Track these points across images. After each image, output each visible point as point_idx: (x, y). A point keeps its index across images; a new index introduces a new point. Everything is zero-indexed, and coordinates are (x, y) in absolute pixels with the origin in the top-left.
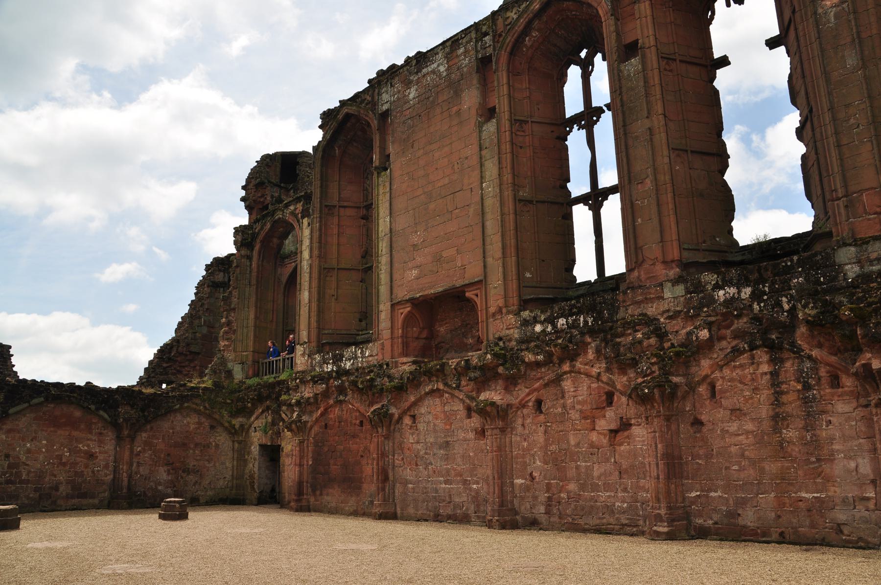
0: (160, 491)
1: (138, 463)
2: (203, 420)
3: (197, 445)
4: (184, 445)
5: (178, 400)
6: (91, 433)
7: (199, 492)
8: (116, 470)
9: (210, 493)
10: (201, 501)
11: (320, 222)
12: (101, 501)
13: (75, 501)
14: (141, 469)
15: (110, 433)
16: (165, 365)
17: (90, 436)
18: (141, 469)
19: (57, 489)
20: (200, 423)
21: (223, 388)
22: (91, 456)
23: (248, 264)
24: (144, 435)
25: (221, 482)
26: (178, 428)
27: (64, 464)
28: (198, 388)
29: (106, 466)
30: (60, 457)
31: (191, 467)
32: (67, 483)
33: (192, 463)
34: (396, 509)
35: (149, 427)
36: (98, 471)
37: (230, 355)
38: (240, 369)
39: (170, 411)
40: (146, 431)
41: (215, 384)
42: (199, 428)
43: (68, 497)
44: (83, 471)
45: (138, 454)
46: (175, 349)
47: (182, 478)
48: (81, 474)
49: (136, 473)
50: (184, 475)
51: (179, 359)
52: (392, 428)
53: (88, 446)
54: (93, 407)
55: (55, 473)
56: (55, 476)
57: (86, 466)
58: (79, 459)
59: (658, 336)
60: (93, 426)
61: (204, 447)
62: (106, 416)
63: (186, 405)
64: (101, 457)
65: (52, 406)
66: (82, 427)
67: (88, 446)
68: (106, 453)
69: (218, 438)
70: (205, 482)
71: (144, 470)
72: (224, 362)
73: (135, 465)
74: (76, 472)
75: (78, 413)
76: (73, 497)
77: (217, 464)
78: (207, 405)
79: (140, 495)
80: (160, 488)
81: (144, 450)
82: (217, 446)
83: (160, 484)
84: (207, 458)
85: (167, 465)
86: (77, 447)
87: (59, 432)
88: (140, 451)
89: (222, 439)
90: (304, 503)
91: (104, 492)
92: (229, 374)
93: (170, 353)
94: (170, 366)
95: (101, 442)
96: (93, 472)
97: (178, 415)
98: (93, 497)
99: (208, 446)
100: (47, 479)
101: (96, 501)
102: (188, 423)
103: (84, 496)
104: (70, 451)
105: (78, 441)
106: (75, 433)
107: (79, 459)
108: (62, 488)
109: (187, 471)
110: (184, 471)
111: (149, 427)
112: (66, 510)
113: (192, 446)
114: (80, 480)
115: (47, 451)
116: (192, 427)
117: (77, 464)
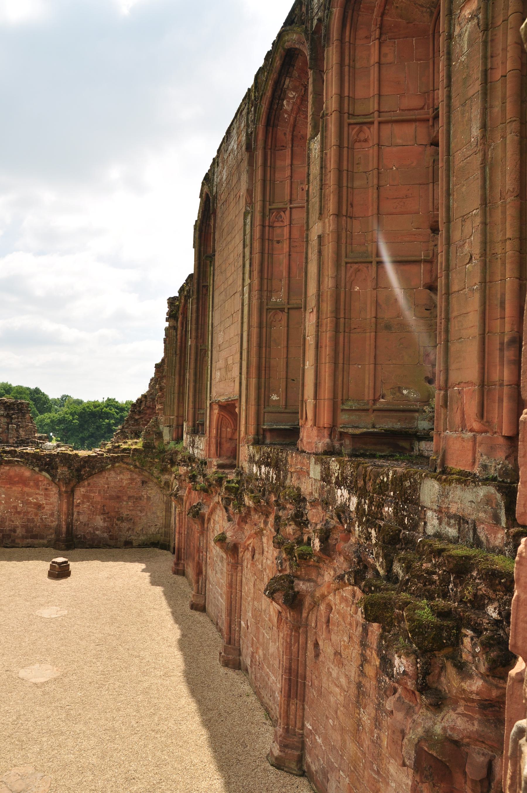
0: (97, 535)
1: (78, 512)
2: (135, 476)
3: (130, 497)
4: (118, 497)
5: (111, 460)
6: (38, 489)
7: (132, 537)
8: (59, 519)
9: (142, 538)
10: (134, 544)
11: (198, 303)
12: (49, 541)
13: (29, 541)
14: (81, 517)
15: (54, 489)
16: (137, 417)
17: (38, 491)
18: (81, 517)
19: (15, 531)
20: (132, 479)
21: (154, 448)
22: (39, 506)
23: (175, 334)
24: (82, 489)
25: (153, 529)
26: (112, 484)
27: (19, 513)
28: (129, 450)
29: (52, 515)
30: (15, 507)
31: (124, 516)
32: (22, 527)
33: (125, 513)
34: (205, 602)
35: (86, 483)
36: (46, 518)
37: (162, 418)
38: (168, 432)
39: (102, 470)
40: (84, 487)
41: (145, 446)
42: (131, 483)
43: (24, 537)
44: (33, 519)
45: (78, 505)
46: (144, 403)
47: (117, 525)
48: (32, 521)
49: (77, 520)
50: (118, 522)
51: (148, 412)
52: (206, 526)
53: (37, 499)
54: (37, 469)
55: (13, 519)
56: (13, 522)
57: (36, 515)
58: (30, 509)
59: (298, 524)
60: (40, 483)
61: (136, 499)
62: (48, 476)
63: (117, 465)
64: (47, 507)
65: (8, 468)
66: (32, 483)
67: (37, 499)
68: (51, 504)
69: (149, 492)
70: (138, 529)
71: (83, 518)
72: (157, 424)
73: (75, 514)
74: (28, 519)
75: (27, 474)
76: (27, 538)
77: (149, 514)
78: (137, 464)
79: (80, 538)
80: (97, 532)
81: (83, 503)
82: (149, 498)
83: (97, 529)
84: (139, 508)
85: (103, 514)
86: (28, 500)
87: (14, 488)
88: (79, 503)
89: (153, 492)
90: (181, 568)
91: (51, 534)
92: (160, 435)
93: (140, 407)
94: (142, 418)
95: (47, 496)
96: (42, 519)
97: (112, 472)
98: (42, 538)
99: (140, 498)
100: (7, 524)
101: (45, 541)
102: (122, 479)
103: (35, 537)
104: (23, 503)
105: (28, 495)
106: (26, 489)
107: (30, 509)
108: (18, 531)
109: (121, 519)
110: (118, 520)
111: (86, 483)
112: (23, 547)
113: (125, 498)
114: (32, 525)
115: (6, 502)
116: (125, 482)
117: (28, 513)
